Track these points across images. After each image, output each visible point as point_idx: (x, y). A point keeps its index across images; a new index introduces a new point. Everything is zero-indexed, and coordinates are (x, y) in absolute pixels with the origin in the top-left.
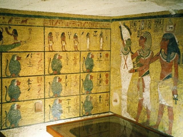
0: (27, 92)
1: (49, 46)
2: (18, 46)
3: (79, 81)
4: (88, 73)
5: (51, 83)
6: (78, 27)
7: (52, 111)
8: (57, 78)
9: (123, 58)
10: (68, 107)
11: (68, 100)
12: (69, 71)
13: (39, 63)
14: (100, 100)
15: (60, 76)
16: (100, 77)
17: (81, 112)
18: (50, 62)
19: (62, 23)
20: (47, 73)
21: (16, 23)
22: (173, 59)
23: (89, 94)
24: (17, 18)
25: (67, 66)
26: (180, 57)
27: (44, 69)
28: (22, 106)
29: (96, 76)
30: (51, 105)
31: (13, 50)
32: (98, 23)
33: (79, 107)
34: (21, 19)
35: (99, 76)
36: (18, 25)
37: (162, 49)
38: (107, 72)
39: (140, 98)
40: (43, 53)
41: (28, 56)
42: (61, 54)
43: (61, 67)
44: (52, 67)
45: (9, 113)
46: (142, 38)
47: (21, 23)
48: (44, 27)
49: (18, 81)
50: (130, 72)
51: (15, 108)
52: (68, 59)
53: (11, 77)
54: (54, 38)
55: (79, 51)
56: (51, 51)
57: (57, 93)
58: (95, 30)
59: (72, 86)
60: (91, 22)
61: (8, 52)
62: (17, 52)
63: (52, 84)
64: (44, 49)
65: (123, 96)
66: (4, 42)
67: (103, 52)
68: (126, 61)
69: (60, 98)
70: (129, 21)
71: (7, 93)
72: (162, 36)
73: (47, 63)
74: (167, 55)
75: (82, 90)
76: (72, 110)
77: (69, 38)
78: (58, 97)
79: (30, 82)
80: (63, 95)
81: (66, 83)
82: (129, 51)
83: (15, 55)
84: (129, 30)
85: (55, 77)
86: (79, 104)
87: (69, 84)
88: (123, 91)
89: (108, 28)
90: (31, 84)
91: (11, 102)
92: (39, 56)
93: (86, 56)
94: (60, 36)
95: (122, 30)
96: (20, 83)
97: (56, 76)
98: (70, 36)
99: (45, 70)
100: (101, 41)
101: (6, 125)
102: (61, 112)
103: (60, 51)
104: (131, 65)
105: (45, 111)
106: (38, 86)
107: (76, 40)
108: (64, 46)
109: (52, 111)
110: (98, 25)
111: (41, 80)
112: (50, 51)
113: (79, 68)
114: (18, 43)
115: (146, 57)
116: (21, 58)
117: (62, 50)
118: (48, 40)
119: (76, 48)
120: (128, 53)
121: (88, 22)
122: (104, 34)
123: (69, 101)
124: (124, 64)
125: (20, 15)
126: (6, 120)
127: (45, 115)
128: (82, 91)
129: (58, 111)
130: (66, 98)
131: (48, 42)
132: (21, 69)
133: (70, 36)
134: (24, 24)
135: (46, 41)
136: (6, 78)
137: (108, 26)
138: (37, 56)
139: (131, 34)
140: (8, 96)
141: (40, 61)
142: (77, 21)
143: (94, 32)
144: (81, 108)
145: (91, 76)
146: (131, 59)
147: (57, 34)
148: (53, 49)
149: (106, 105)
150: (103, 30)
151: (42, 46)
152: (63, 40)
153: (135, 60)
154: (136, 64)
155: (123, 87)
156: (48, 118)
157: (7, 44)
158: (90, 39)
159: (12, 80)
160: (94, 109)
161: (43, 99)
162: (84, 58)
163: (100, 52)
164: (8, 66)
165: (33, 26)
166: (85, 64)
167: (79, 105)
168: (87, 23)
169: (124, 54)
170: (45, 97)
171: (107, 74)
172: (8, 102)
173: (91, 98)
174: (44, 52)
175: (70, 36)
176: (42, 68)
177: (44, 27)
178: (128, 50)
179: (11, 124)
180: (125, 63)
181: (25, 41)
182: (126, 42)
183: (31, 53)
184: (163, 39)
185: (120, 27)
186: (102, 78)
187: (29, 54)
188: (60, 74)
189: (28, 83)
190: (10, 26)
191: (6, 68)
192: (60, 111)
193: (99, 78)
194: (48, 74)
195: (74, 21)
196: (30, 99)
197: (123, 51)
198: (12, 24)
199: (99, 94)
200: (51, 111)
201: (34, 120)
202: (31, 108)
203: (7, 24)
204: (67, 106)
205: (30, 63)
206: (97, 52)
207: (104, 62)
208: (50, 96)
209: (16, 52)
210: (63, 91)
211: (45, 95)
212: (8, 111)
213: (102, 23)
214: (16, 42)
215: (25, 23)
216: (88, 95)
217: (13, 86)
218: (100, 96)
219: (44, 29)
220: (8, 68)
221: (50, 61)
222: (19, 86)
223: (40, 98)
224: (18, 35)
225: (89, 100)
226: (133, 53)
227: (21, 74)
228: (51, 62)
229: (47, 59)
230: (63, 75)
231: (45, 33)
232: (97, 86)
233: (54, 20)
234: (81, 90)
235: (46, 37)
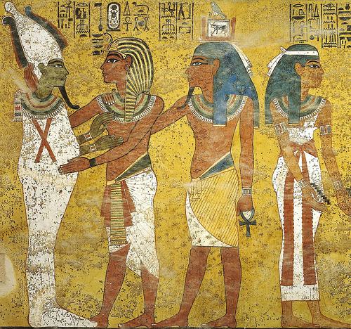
9: (28, 127)
22: (236, 114)
26: (256, 106)
37: (196, 89)
39: (113, 249)
46: (113, 57)
50: (66, 169)
65: (31, 258)
68: (44, 135)
82: (60, 102)
84: (51, 29)
88: (33, 240)
95: (20, 32)
104: (69, 148)
115: (137, 114)
120: (56, 107)
124: (38, 146)
139: (62, 44)
154: (91, 142)
155: (32, 227)
169: (33, 113)
178: (52, 98)
180: (40, 141)
182: (43, 72)
185: (10, 21)
197: (27, 103)
226: (77, 107)
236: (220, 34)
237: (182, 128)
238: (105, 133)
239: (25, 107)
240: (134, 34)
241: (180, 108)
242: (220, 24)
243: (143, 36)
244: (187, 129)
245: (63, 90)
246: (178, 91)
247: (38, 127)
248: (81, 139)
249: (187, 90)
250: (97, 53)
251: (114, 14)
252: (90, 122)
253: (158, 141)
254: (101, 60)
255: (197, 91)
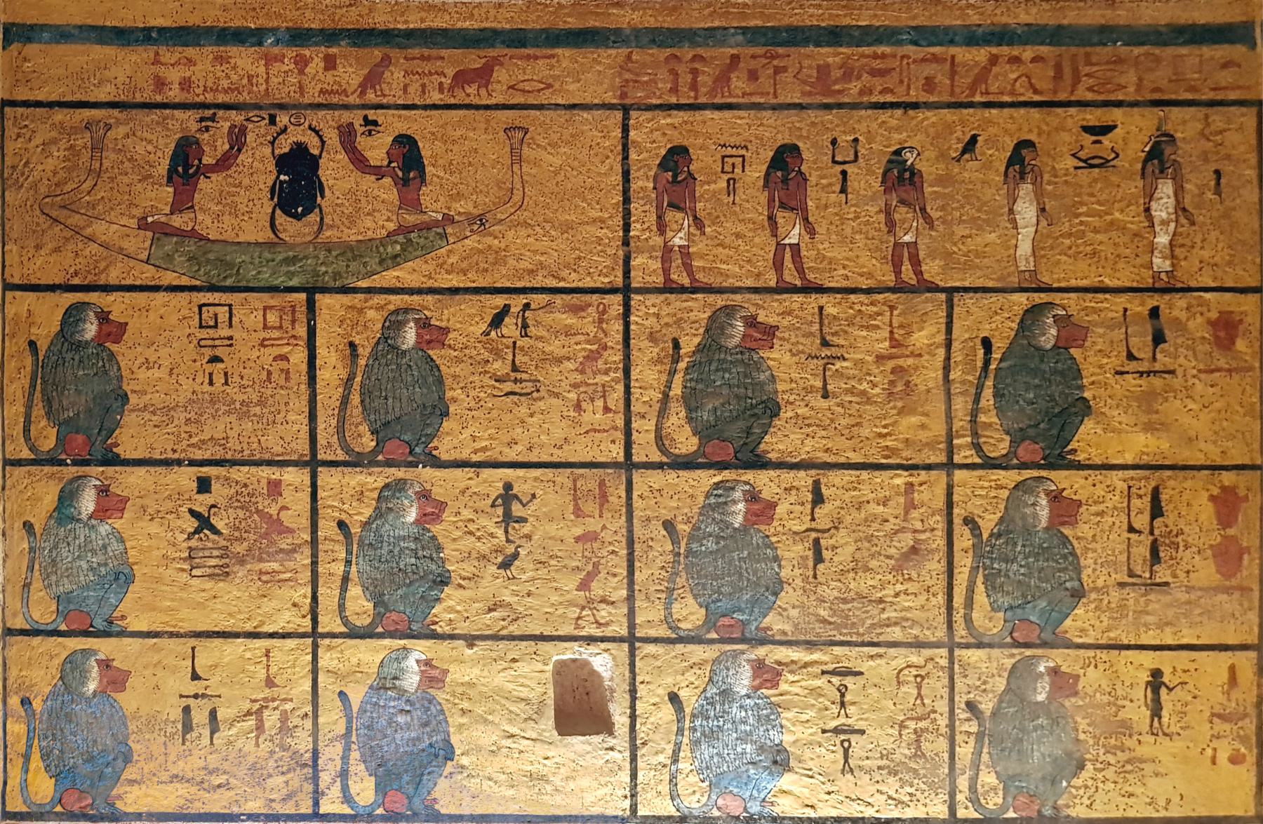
0: (492, 582)
1: (667, 250)
2: (427, 250)
3: (940, 534)
4: (1028, 474)
5: (684, 528)
6: (924, 97)
7: (696, 743)
8: (738, 494)
10: (837, 731)
11: (834, 673)
12: (842, 443)
13: (582, 372)
14: (1156, 712)
15: (765, 482)
16: (1157, 510)
17: (963, 783)
18: (672, 373)
19: (778, 70)
20: (645, 449)
21: (414, 88)
23: (1045, 644)
24: (428, 58)
25: (824, 404)
27: (628, 423)
28: (458, 674)
29: (1115, 499)
30: (690, 699)
31: (389, 277)
32: (1120, 61)
33: (943, 744)
34: (453, 60)
35: (1142, 504)
36: (425, 107)
38: (1228, 478)
40: (619, 298)
41: (497, 321)
42: (769, 311)
43: (772, 409)
44: (691, 401)
45: (362, 710)
47: (451, 89)
48: (626, 110)
49: (425, 495)
51: (411, 681)
52: (826, 352)
53: (378, 464)
54: (709, 188)
55: (938, 289)
56: (683, 290)
57: (740, 610)
58: (1093, 117)
59: (873, 564)
60: (1044, 50)
61: (355, 290)
62: (420, 291)
63: (691, 538)
64: (627, 273)
66: (327, 220)
67: (1180, 301)
69: (761, 651)
71: (354, 568)
73: (647, 374)
75: (969, 603)
76: (880, 763)
77: (838, 188)
78: (743, 640)
79: (517, 509)
80: (788, 628)
81: (817, 542)
83: (406, 311)
85: (717, 486)
86: (943, 722)
87: (842, 549)
89: (1233, 96)
90: (522, 520)
91: (381, 636)
92: (587, 324)
93: (1003, 330)
94: (756, 172)
96: (442, 506)
97: (726, 475)
98: (850, 169)
99: (634, 425)
100: (1163, 207)
101: (345, 789)
102: (780, 761)
103: (755, 290)
105: (641, 736)
106: (577, 539)
107: (902, 202)
108: (795, 248)
109: (696, 743)
110: (1130, 78)
111: (604, 497)
112: (670, 288)
113: (939, 428)
114: (427, 227)
116: (445, 331)
117: (780, 277)
118: (659, 207)
119: (907, 267)
121: (1016, 51)
122: (1189, 145)
123: (849, 681)
125: (445, 32)
126: (345, 758)
127: (640, 764)
128: (968, 620)
129: (749, 748)
130: (816, 656)
131: (659, 217)
132: (445, 414)
133: (850, 169)
134: (472, 93)
135: (643, 212)
136: (345, 464)
137: (1225, 77)
138: (569, 320)
140: (355, 591)
141: (592, 357)
142: (910, 49)
143: (1088, 129)
144: (965, 751)
145: (1056, 498)
147: (732, 160)
148: (699, 276)
149: (1223, 756)
150: (1175, 112)
151: (610, 251)
152: (783, 206)
156: (665, 788)
157: (351, 236)
158: (1039, 195)
159: (380, 483)
160: (1085, 775)
161: (621, 640)
162: (987, 344)
163: (1153, 301)
164: (356, 386)
165: (540, 107)
166: (997, 395)
167: (943, 730)
168: (1016, 60)
170: (632, 626)
171: (1224, 489)
172: (355, 633)
173: (1062, 682)
174: (626, 290)
175: (844, 173)
176: (607, 409)
177: (626, 110)
179: (381, 789)
181: (476, 212)
183: (520, 301)
186: (1170, 518)
187: (506, 310)
188: (760, 463)
189: (500, 511)
190: (372, 114)
191: (345, 401)
192: (761, 749)
193: (1141, 521)
194: (656, 457)
195: (887, 49)
196: (514, 629)
198: (385, 101)
199: (1149, 660)
200: (686, 740)
201: (549, 788)
202: (524, 692)
203: (353, 99)
204: (833, 724)
205: (515, 369)
206: (1122, 300)
207: (1199, 386)
208: (674, 628)
209: (411, 291)
210: (788, 597)
211: (631, 614)
212: (357, 696)
213: (1158, 60)
214: (411, 219)
215: (475, 86)
216: (1028, 652)
217: (394, 528)
218: (1156, 674)
219: (625, 129)
220: (355, 399)
221: (676, 359)
222: (436, 529)
223: (598, 632)
224: (429, 169)
225: (1041, 697)
227: (445, 448)
228: (682, 365)
229: (644, 352)
230: (788, 477)
231: (633, 156)
232: (1122, 585)
233: (700, 51)
234: (958, 600)
235: (642, 183)
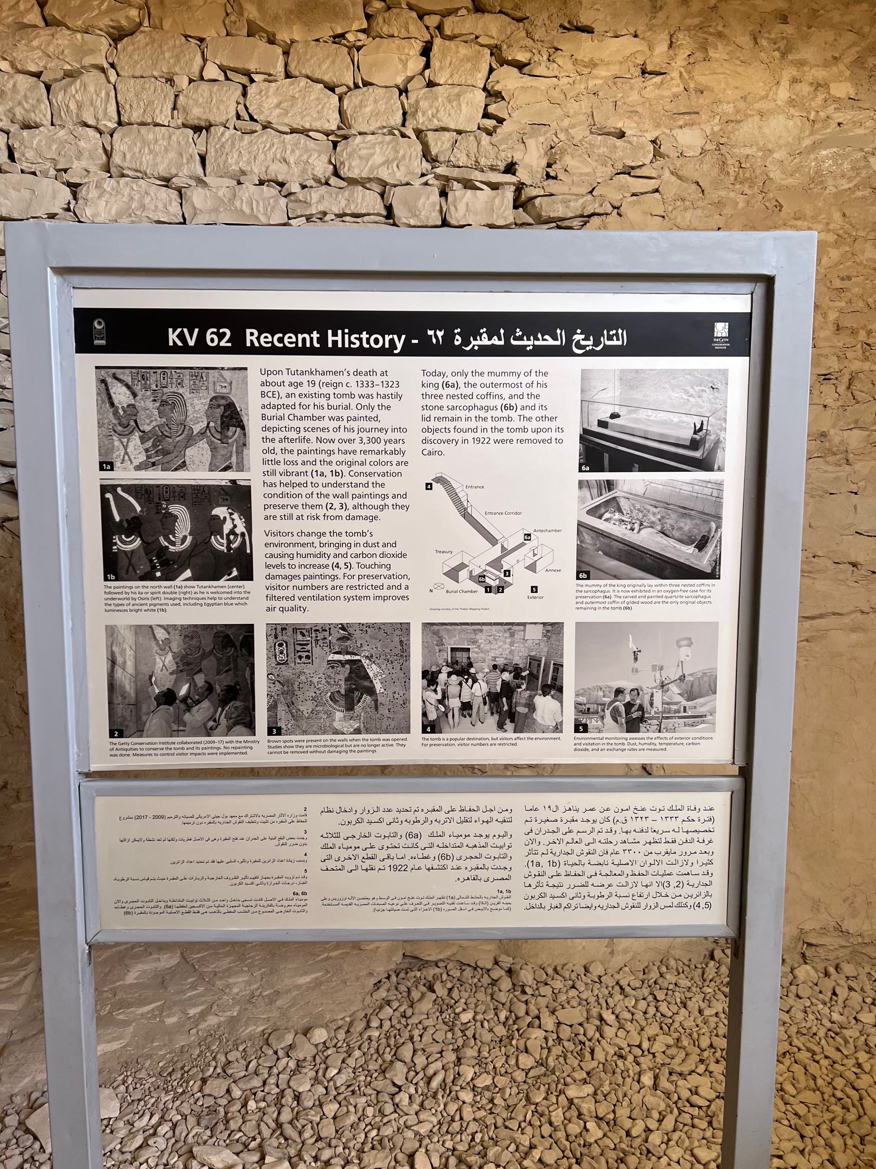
9: (117, 443)
68: (126, 448)
70: (127, 371)
72: (209, 400)
74: (221, 433)
84: (128, 386)
124: (122, 454)
139: (135, 395)
146: (139, 443)
153: (149, 444)
182: (124, 411)
184: (211, 407)
226: (144, 432)
236: (224, 391)
237: (203, 445)
238: (160, 447)
239: (115, 431)
240: (174, 389)
241: (202, 434)
242: (224, 385)
243: (181, 391)
244: (206, 446)
245: (136, 422)
246: (201, 424)
247: (122, 443)
248: (147, 450)
249: (206, 423)
250: (155, 400)
251: (164, 378)
252: (152, 441)
253: (189, 452)
254: (158, 404)
255: (212, 424)
